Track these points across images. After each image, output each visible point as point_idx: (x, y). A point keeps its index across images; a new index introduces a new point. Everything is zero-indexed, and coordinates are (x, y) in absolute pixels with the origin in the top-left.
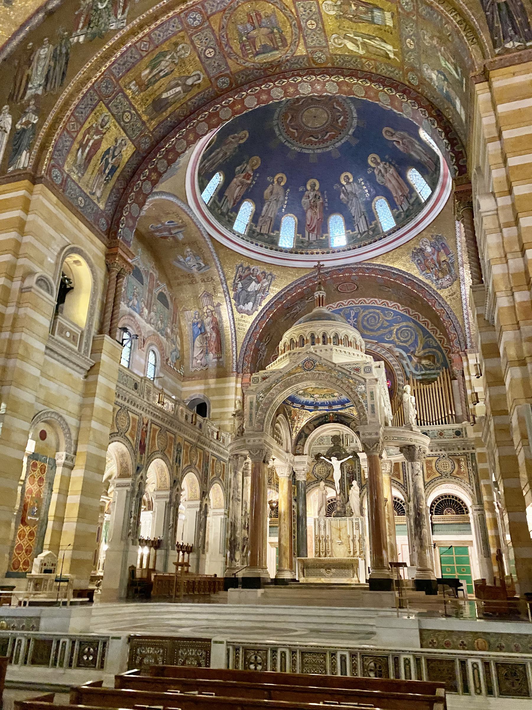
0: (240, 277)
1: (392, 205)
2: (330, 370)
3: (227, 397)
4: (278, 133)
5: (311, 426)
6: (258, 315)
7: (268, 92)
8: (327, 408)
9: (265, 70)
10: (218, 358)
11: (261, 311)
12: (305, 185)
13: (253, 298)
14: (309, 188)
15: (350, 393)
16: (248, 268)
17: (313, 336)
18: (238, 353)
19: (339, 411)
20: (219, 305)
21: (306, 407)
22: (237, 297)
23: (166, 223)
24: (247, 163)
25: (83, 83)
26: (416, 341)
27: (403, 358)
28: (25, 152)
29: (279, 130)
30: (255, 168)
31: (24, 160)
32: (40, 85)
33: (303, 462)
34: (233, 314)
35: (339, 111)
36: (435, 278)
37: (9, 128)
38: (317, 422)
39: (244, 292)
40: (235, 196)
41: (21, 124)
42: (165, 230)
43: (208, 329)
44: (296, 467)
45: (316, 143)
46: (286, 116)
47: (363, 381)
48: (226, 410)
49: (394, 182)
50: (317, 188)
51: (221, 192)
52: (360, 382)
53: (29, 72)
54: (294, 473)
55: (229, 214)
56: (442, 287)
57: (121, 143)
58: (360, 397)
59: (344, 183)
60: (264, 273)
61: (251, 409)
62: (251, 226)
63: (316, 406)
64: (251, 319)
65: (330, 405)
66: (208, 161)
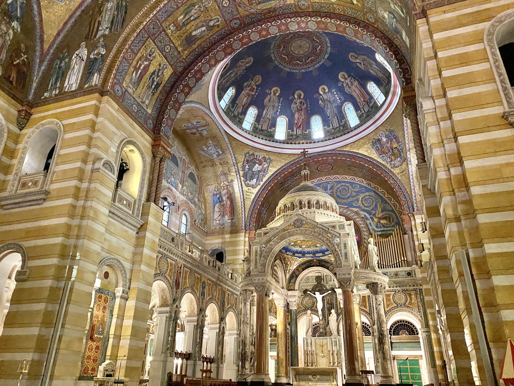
0: (247, 161)
1: (357, 108)
2: (314, 228)
3: (238, 248)
4: (273, 58)
5: (300, 269)
6: (261, 188)
7: (267, 29)
8: (311, 255)
9: (265, 15)
10: (232, 219)
11: (262, 186)
12: (294, 95)
14: (296, 97)
15: (329, 244)
16: (253, 154)
17: (300, 203)
18: (246, 216)
19: (321, 258)
20: (232, 181)
21: (296, 255)
22: (245, 175)
23: (195, 123)
24: (252, 80)
25: (137, 25)
26: (376, 206)
27: (367, 219)
28: (96, 74)
29: (275, 57)
30: (258, 84)
31: (96, 79)
32: (107, 28)
33: (295, 296)
34: (242, 188)
35: (317, 42)
36: (389, 160)
37: (85, 58)
38: (305, 266)
39: (250, 171)
40: (244, 103)
41: (93, 55)
42: (193, 128)
43: (224, 198)
44: (290, 300)
45: (301, 65)
46: (279, 47)
47: (338, 235)
48: (237, 257)
49: (357, 91)
50: (302, 97)
51: (234, 101)
52: (336, 236)
53: (100, 19)
54: (288, 304)
55: (240, 116)
56: (395, 167)
57: (163, 67)
58: (336, 247)
59: (321, 93)
60: (264, 157)
61: (256, 256)
62: (255, 124)
63: (303, 254)
64: (255, 191)
65: (314, 253)
66: (224, 79)
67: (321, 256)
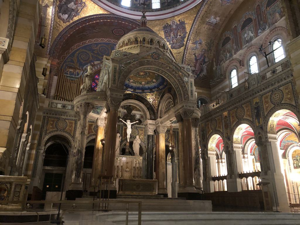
13: (69, 13)
19: (139, 94)
36: (171, 42)
39: (65, 6)
47: (187, 75)
52: (185, 75)
64: (64, 25)
65: (135, 89)
67: (140, 93)
